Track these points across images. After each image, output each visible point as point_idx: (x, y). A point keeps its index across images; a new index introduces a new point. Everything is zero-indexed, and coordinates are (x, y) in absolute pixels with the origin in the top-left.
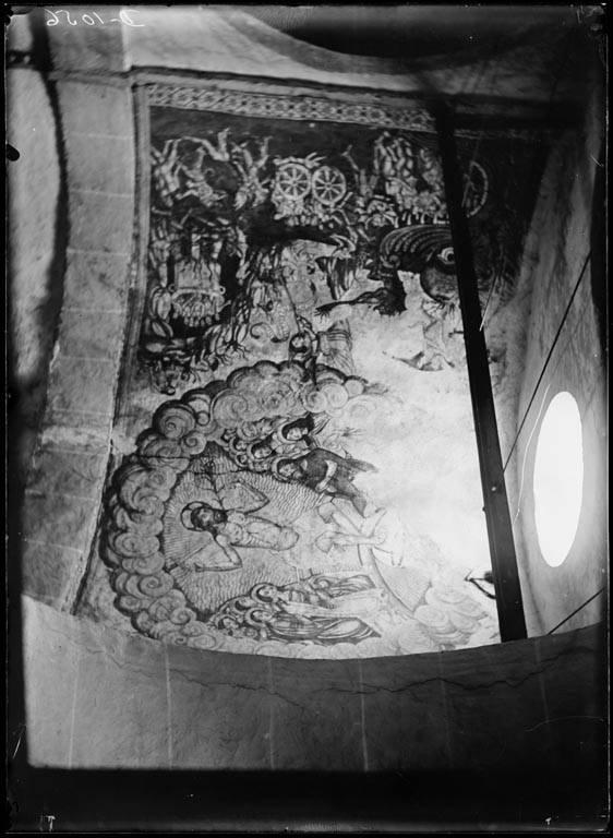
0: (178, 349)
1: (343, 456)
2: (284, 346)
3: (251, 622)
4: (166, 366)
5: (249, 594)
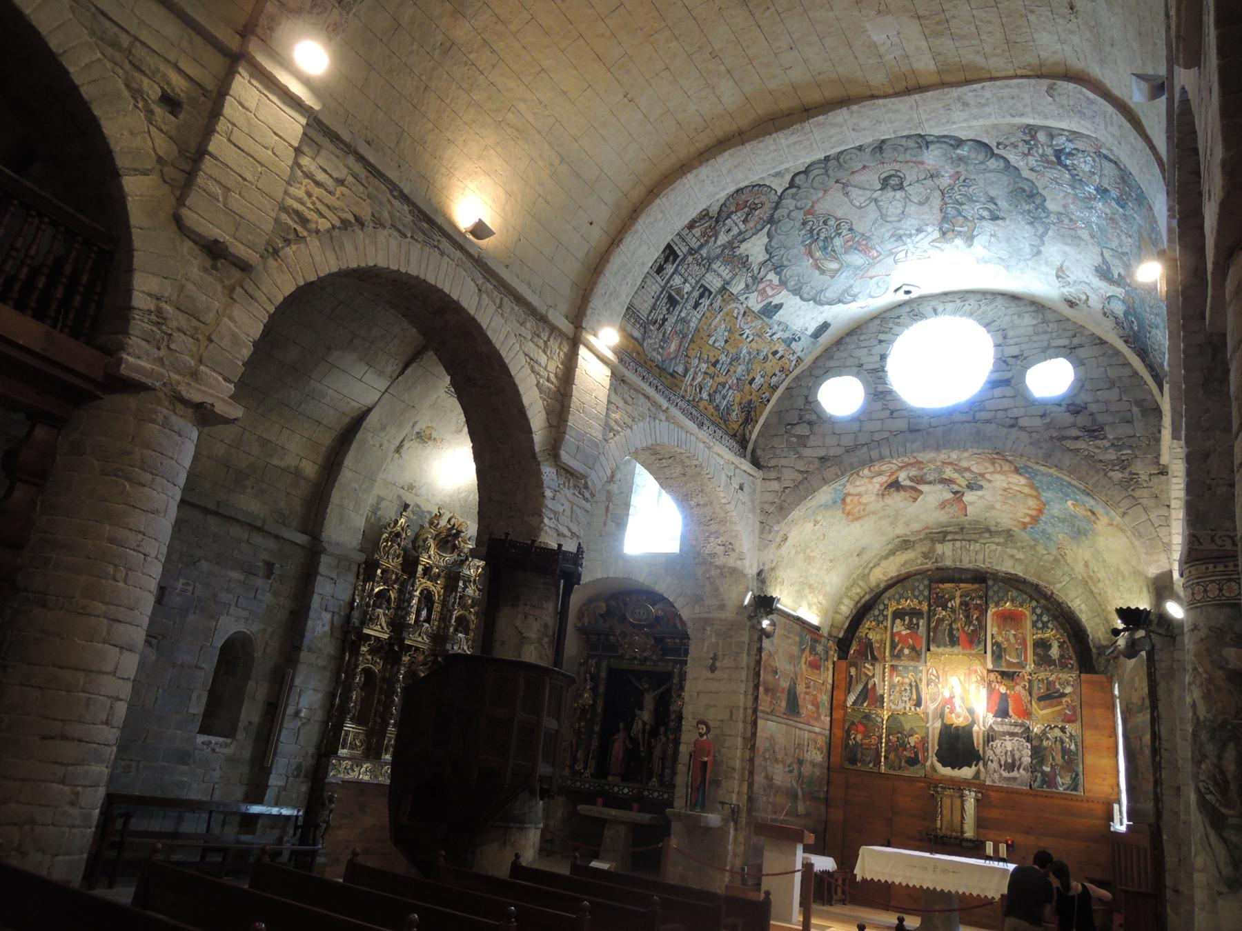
1: (975, 233)
2: (1061, 210)
3: (815, 232)
4: (1026, 142)
5: (837, 219)
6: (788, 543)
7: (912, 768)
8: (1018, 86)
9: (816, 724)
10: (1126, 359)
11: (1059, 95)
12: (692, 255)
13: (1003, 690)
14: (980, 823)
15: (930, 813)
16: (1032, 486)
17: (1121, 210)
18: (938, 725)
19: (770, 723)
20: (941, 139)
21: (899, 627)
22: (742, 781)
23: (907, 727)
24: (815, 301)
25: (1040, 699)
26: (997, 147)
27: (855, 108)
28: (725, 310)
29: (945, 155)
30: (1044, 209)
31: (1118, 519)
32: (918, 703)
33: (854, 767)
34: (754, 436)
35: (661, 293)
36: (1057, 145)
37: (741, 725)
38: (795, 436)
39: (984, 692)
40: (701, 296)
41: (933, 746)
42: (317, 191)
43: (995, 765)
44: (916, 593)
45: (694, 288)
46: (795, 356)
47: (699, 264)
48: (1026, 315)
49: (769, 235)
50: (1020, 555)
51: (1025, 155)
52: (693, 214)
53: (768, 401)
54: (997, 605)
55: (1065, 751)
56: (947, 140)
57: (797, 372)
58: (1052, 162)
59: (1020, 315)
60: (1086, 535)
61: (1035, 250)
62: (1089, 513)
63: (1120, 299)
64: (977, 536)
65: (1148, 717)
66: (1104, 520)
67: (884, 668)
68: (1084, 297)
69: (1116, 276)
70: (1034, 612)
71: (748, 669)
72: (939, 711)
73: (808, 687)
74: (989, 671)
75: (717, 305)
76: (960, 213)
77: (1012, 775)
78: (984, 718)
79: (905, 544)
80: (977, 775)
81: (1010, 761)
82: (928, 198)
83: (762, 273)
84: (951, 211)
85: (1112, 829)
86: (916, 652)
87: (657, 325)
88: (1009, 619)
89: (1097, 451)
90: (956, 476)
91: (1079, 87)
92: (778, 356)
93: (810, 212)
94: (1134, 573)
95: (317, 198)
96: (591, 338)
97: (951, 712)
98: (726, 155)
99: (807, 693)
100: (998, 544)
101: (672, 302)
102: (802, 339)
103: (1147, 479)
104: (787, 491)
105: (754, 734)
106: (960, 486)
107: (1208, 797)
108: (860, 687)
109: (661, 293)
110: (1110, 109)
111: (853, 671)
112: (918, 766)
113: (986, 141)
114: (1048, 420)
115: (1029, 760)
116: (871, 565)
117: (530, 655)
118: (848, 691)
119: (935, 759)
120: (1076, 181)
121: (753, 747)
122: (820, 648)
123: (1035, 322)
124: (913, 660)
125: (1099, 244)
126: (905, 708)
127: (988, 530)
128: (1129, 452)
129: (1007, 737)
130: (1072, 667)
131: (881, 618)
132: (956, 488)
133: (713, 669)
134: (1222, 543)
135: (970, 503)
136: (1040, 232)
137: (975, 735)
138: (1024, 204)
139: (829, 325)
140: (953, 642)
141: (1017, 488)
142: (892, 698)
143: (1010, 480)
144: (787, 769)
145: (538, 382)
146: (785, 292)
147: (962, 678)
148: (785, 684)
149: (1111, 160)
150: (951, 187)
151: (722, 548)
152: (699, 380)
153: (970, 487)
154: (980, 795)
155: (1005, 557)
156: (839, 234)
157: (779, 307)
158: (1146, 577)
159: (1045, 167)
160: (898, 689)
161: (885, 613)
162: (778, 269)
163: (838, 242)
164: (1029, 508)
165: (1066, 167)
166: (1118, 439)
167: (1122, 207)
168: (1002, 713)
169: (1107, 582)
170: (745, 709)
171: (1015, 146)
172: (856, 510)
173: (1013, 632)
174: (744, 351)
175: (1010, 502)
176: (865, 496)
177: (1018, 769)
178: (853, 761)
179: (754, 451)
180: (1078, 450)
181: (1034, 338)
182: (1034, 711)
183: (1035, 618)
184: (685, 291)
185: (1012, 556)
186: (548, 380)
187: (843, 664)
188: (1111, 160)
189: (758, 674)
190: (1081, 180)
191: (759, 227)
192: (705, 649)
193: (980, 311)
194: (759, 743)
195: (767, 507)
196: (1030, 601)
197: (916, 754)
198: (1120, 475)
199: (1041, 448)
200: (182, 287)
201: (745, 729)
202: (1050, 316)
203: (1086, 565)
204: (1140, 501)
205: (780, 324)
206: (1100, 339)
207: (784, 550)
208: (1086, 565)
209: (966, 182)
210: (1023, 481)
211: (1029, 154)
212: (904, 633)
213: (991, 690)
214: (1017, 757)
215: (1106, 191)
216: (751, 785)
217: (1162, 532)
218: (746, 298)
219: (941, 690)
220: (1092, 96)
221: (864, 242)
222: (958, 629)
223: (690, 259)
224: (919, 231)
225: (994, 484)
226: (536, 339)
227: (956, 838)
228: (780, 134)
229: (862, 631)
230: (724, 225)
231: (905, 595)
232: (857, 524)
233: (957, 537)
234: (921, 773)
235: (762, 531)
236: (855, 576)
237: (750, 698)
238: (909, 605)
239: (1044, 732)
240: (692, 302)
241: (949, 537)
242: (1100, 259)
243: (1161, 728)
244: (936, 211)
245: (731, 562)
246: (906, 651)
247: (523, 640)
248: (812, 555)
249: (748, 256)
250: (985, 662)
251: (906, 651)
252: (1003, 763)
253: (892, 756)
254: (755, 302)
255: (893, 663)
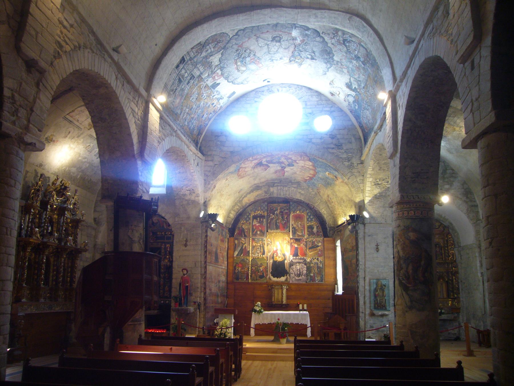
0: (339, 38)
1: (303, 63)
2: (339, 60)
4: (334, 34)
5: (250, 50)
6: (215, 189)
7: (261, 279)
8: (338, 14)
9: (223, 265)
10: (350, 118)
11: (353, 21)
12: (190, 60)
13: (296, 246)
14: (288, 298)
15: (270, 296)
16: (314, 166)
17: (363, 66)
18: (271, 261)
19: (210, 267)
20: (301, 27)
21: (255, 223)
22: (201, 292)
23: (259, 263)
24: (232, 83)
25: (310, 248)
26: (322, 33)
27: (273, 9)
28: (198, 85)
29: (301, 32)
30: (333, 59)
31: (346, 180)
32: (264, 254)
33: (238, 281)
34: (200, 141)
35: (176, 77)
36: (345, 37)
37: (200, 269)
38: (219, 141)
39: (289, 247)
40: (191, 79)
41: (270, 270)
42: (64, 31)
43: (293, 275)
44: (262, 208)
45: (188, 75)
46: (220, 105)
47: (192, 65)
48: (314, 97)
49: (222, 54)
50: (303, 192)
51: (332, 38)
52: (196, 43)
53: (207, 125)
54: (294, 212)
55: (318, 268)
56: (303, 27)
57: (219, 112)
58: (341, 43)
59: (312, 96)
60: (330, 185)
61: (324, 73)
62: (334, 177)
63: (352, 96)
64: (286, 184)
65: (355, 253)
66: (340, 180)
67: (250, 240)
68: (338, 93)
69: (353, 88)
70: (307, 215)
71: (201, 245)
72: (272, 256)
73: (220, 250)
74: (291, 239)
75: (196, 83)
76: (299, 55)
77: (299, 278)
78: (289, 257)
79: (257, 187)
80: (286, 280)
81: (299, 273)
82: (289, 47)
83: (216, 69)
84: (296, 53)
85: (335, 294)
86: (262, 232)
87: (173, 92)
88: (298, 218)
89: (340, 154)
90: (285, 161)
91: (361, 20)
92: (214, 105)
93: (241, 46)
94: (349, 200)
95: (65, 34)
96: (154, 100)
97: (277, 256)
98: (216, 20)
99: (220, 253)
100: (294, 188)
101: (180, 81)
102: (224, 98)
103: (356, 165)
104: (216, 166)
105: (205, 272)
106: (285, 164)
107: (403, 281)
108: (239, 248)
109: (176, 77)
110: (371, 32)
111: (236, 242)
112: (264, 278)
113: (319, 30)
114: (323, 141)
115: (306, 272)
116: (243, 196)
117: (137, 248)
118: (235, 251)
119: (270, 275)
120: (348, 52)
121: (205, 278)
122: (224, 233)
123: (317, 100)
124: (261, 236)
125: (350, 75)
126: (258, 256)
127: (291, 182)
128: (351, 155)
129: (298, 264)
130: (321, 236)
131: (248, 219)
132: (283, 165)
133: (186, 245)
134: (410, 198)
135: (287, 171)
136: (328, 67)
137: (286, 264)
138: (325, 56)
139: (235, 93)
140: (277, 228)
141: (307, 166)
142: (253, 252)
143: (306, 163)
144: (216, 285)
145: (135, 121)
146: (222, 78)
147: (281, 242)
148: (214, 250)
149: (364, 48)
150: (300, 45)
151: (189, 192)
152: (185, 116)
153: (289, 165)
154: (288, 287)
155: (297, 193)
156: (249, 56)
157: (218, 84)
158: (355, 202)
159: (337, 44)
160: (255, 248)
161: (249, 217)
162: (222, 69)
163: (248, 59)
164: (310, 174)
165: (346, 46)
166: (347, 149)
167: (364, 65)
168: (296, 255)
169: (336, 203)
170: (201, 262)
171: (329, 34)
172: (242, 174)
173: (300, 223)
174: (202, 103)
175: (303, 171)
176: (247, 168)
177: (302, 276)
178: (237, 279)
179: (200, 147)
180: (333, 153)
181: (317, 106)
182: (307, 253)
183: (308, 217)
184: (185, 76)
185: (300, 193)
186: (138, 120)
187: (232, 239)
188: (364, 48)
189: (206, 247)
190: (350, 52)
191: (219, 50)
192: (182, 237)
193: (296, 93)
194: (208, 276)
195: (207, 173)
196: (306, 211)
197: (263, 273)
198: (348, 164)
199: (320, 152)
200: (21, 84)
201: (201, 270)
202: (323, 98)
203: (328, 196)
204: (354, 173)
205: (217, 91)
206: (341, 109)
207: (213, 192)
208: (328, 196)
209: (306, 44)
210: (311, 164)
211: (333, 38)
212: (257, 225)
213: (292, 246)
214: (301, 271)
215: (359, 57)
216: (205, 293)
217: (361, 185)
218: (207, 80)
219: (273, 247)
220: (365, 24)
221: (258, 60)
222: (279, 223)
223: (189, 62)
224: (281, 59)
225: (299, 164)
226: (134, 100)
227: (280, 304)
228: (241, 15)
229: (240, 225)
230: (206, 48)
231: (258, 209)
232: (241, 180)
233: (279, 185)
234: (265, 281)
235: (205, 184)
236: (236, 201)
237: (203, 257)
238: (259, 213)
239: (311, 261)
240: (187, 82)
241: (276, 185)
242: (349, 81)
243: (359, 257)
244: (290, 53)
245: (193, 198)
246: (258, 232)
247: (132, 242)
248: (223, 193)
249: (212, 62)
250: (289, 235)
251: (258, 232)
252: (296, 274)
253: (253, 275)
254: (210, 82)
255: (253, 237)
